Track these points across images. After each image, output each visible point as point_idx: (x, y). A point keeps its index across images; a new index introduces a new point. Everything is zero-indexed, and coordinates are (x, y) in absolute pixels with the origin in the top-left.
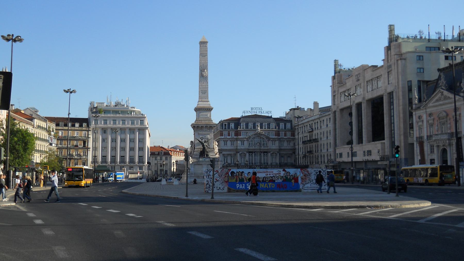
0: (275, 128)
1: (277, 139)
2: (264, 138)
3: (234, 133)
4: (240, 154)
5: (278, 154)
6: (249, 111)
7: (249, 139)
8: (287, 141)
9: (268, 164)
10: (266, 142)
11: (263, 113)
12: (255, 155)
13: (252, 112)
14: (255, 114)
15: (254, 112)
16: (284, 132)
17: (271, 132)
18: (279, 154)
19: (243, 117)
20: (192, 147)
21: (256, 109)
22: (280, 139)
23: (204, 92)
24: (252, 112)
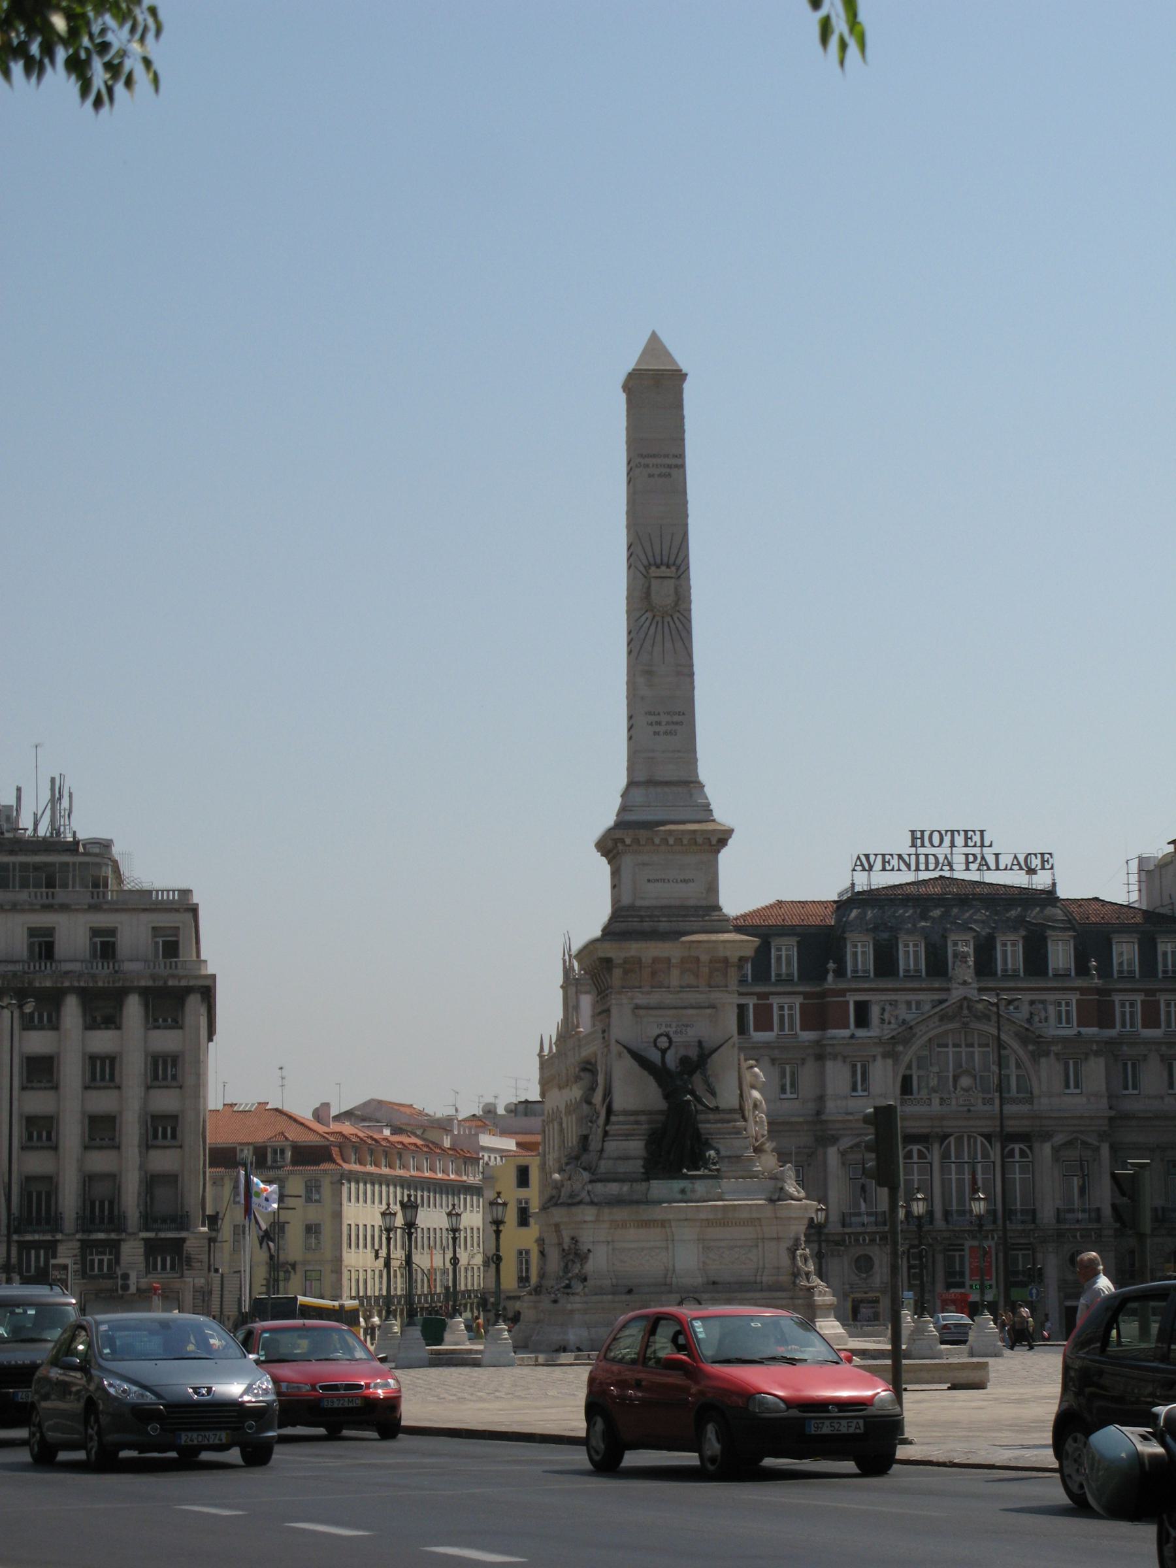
0: (1082, 969)
1: (1095, 1047)
3: (800, 1004)
4: (843, 1154)
5: (1105, 1150)
6: (900, 856)
8: (1163, 1058)
9: (1039, 1215)
10: (1018, 1066)
11: (993, 866)
12: (945, 1156)
13: (922, 859)
14: (936, 874)
15: (932, 859)
16: (1139, 998)
17: (1051, 997)
18: (1114, 1149)
19: (855, 900)
20: (589, 1103)
21: (947, 839)
22: (1110, 1042)
23: (664, 718)
24: (922, 859)
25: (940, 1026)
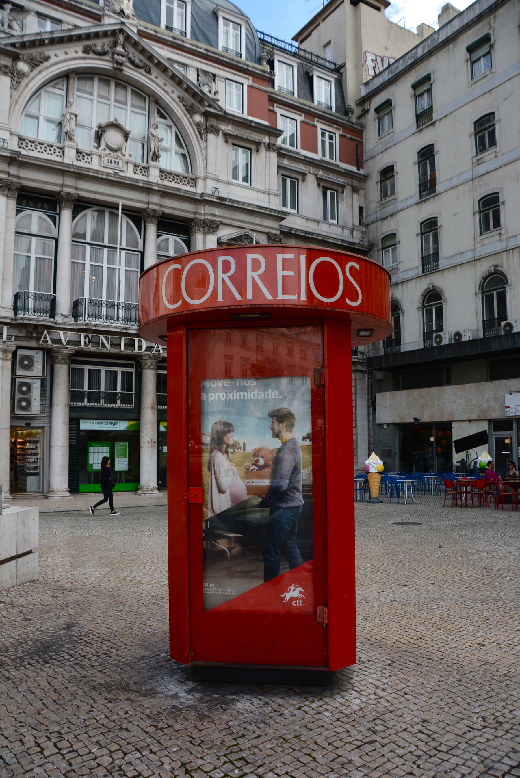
2: (166, 98)
7: (23, 67)
25: (84, 58)
